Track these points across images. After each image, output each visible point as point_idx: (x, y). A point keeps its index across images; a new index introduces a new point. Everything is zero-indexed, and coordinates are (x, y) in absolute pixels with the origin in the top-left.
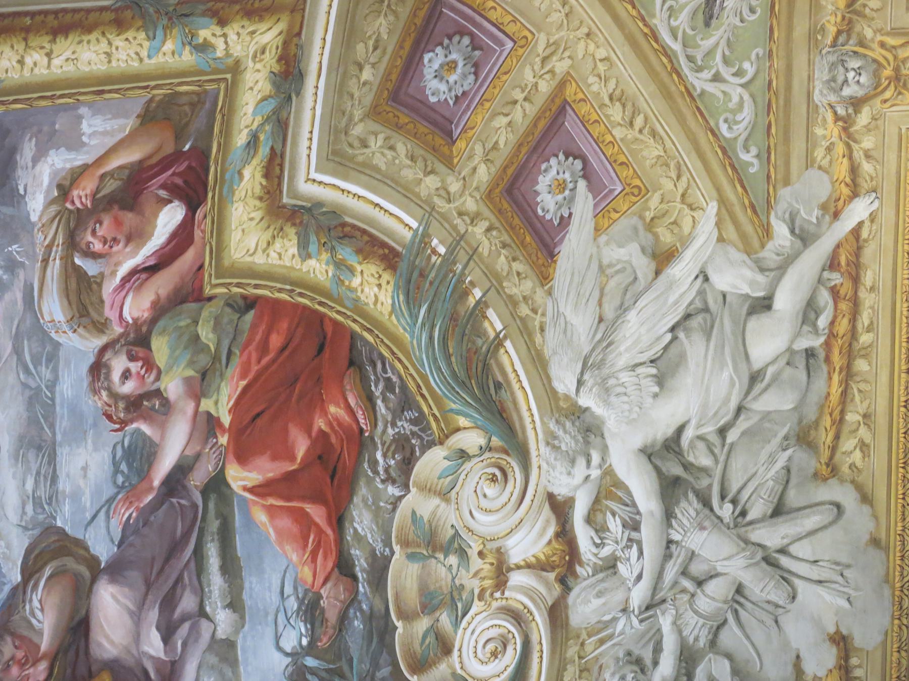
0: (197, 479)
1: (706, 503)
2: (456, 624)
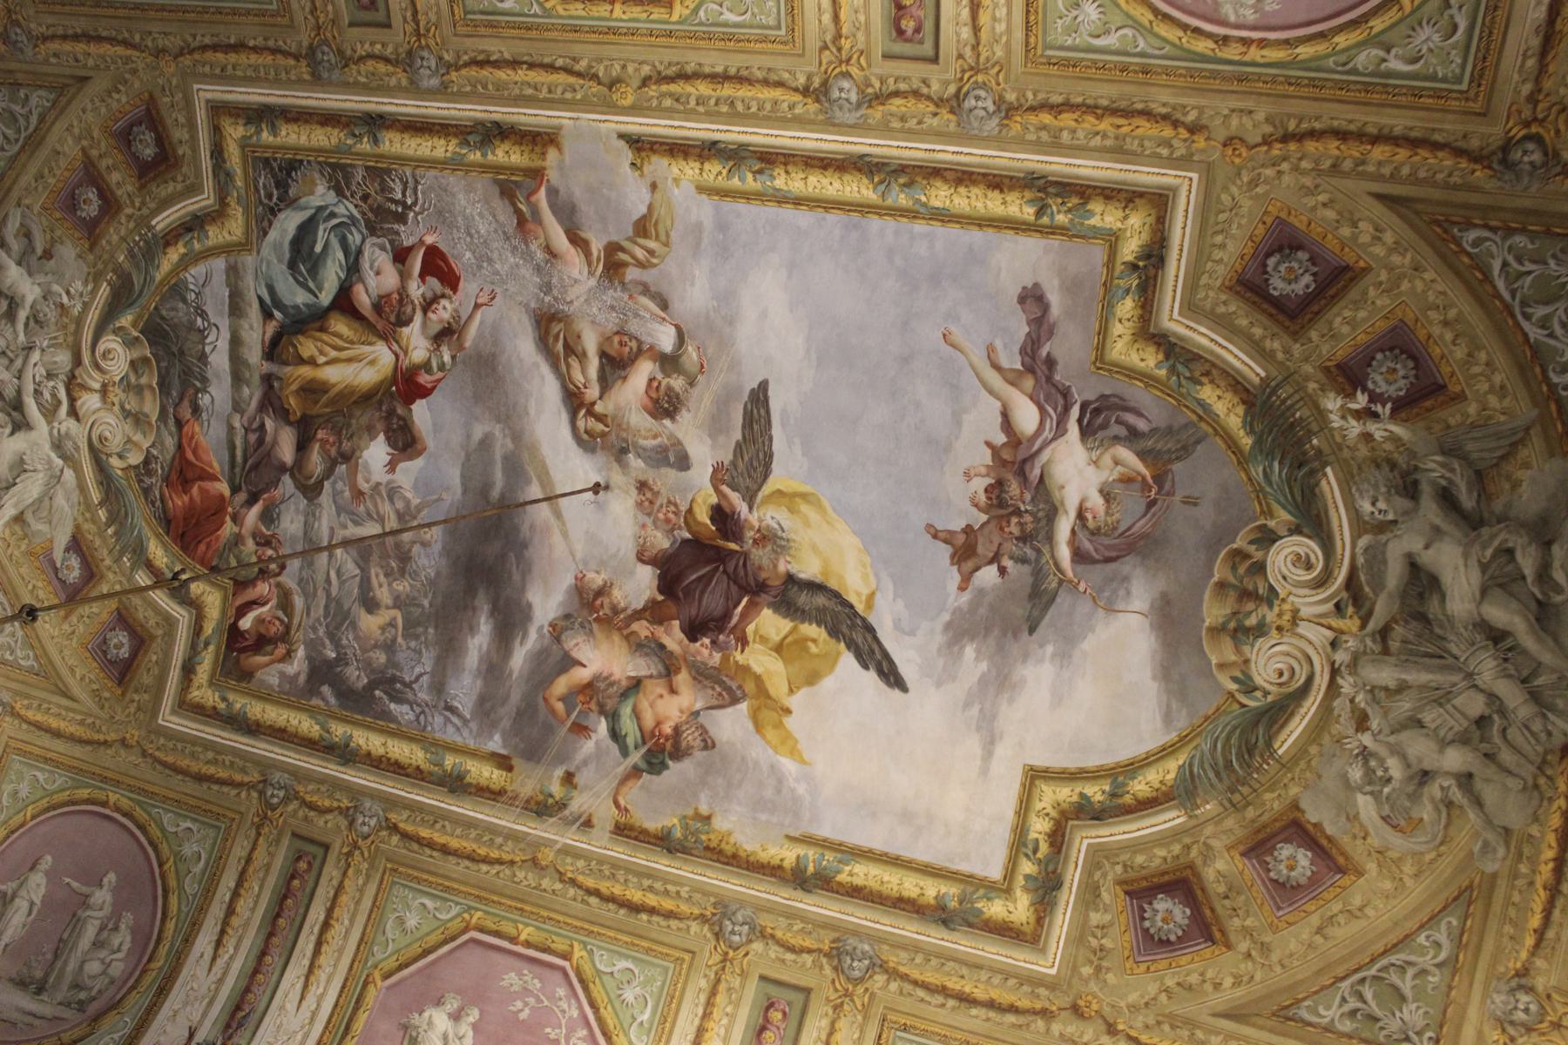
0: (242, 497)
2: (127, 375)
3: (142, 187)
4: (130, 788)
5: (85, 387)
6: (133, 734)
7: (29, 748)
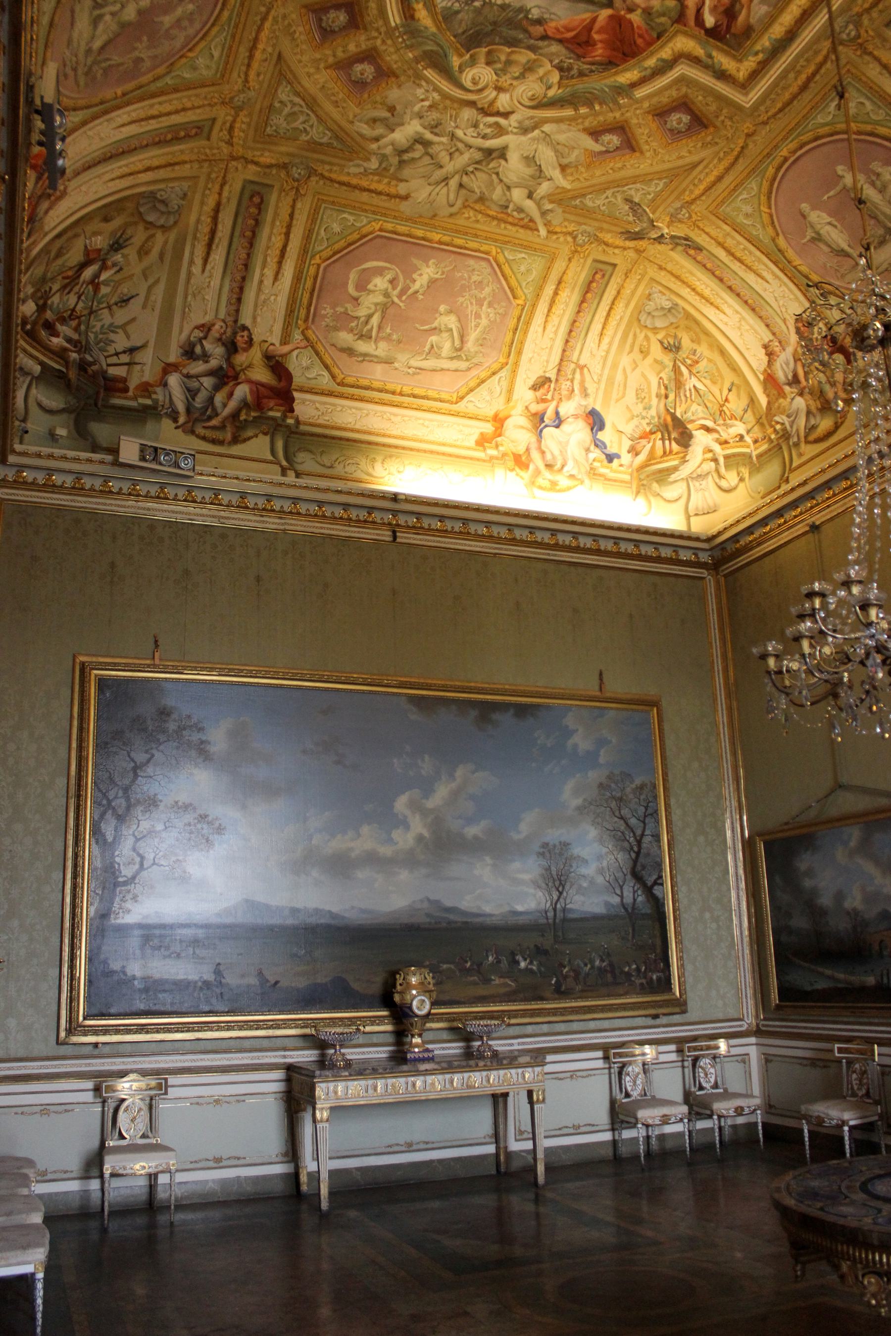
1: (477, 163)
3: (365, 29)
4: (785, 139)
5: (492, 103)
6: (748, 127)
7: (720, 199)
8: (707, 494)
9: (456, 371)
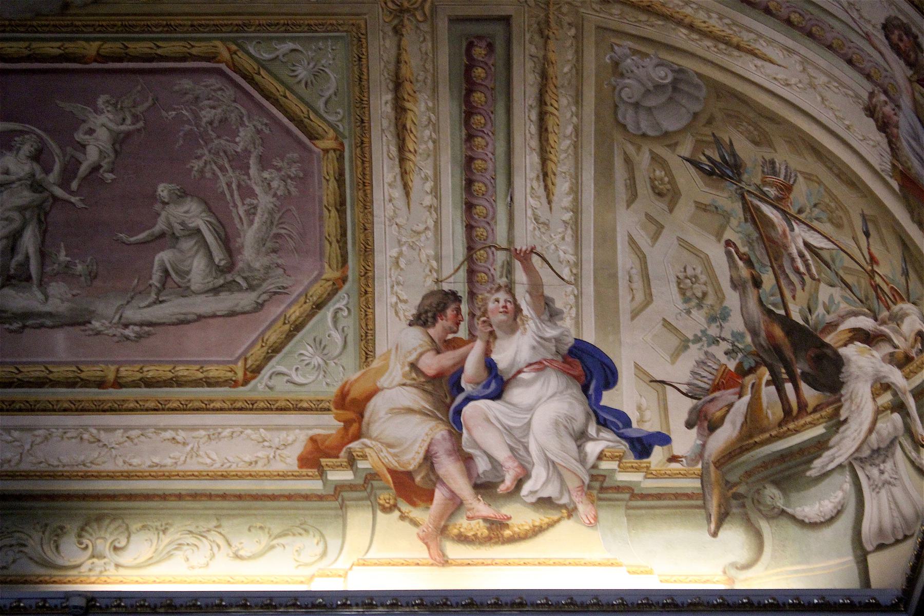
8: (897, 492)
9: (232, 314)
